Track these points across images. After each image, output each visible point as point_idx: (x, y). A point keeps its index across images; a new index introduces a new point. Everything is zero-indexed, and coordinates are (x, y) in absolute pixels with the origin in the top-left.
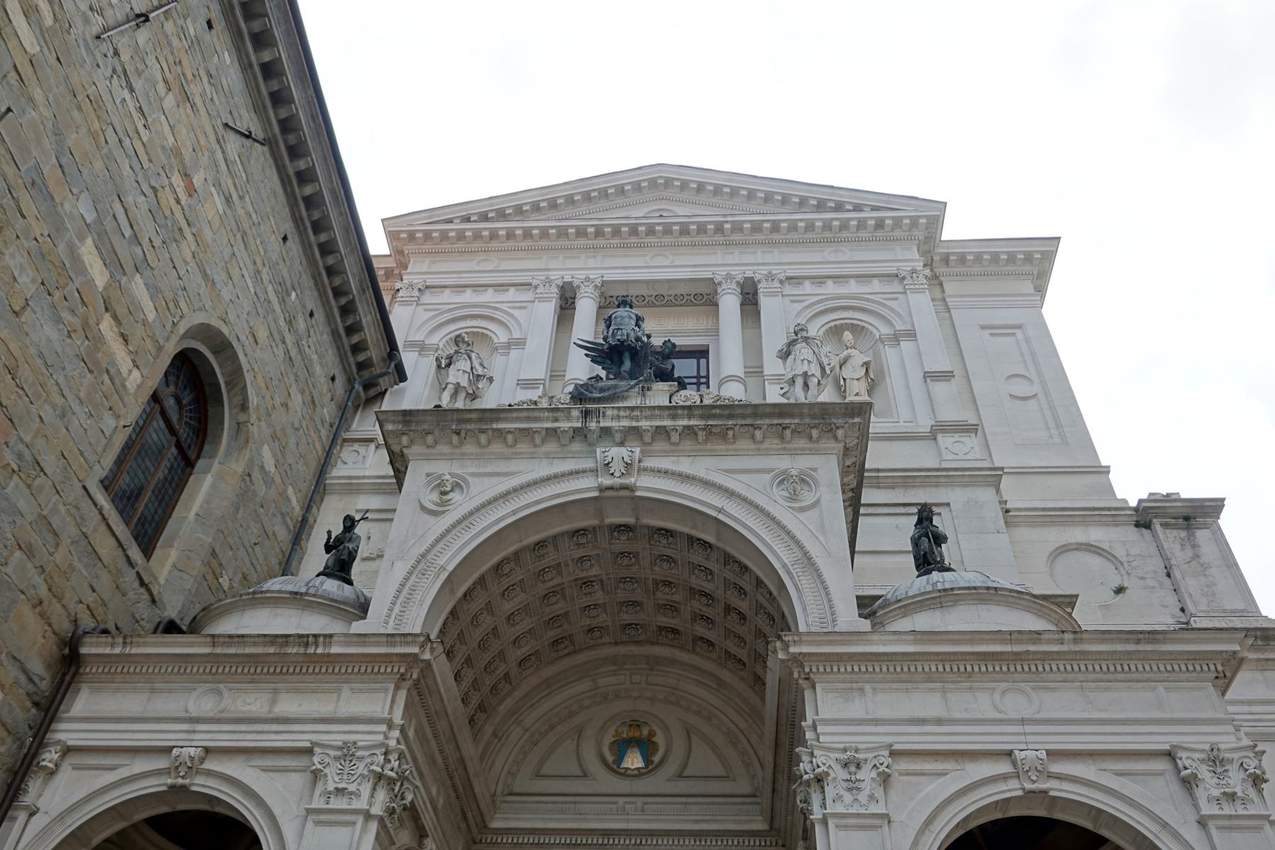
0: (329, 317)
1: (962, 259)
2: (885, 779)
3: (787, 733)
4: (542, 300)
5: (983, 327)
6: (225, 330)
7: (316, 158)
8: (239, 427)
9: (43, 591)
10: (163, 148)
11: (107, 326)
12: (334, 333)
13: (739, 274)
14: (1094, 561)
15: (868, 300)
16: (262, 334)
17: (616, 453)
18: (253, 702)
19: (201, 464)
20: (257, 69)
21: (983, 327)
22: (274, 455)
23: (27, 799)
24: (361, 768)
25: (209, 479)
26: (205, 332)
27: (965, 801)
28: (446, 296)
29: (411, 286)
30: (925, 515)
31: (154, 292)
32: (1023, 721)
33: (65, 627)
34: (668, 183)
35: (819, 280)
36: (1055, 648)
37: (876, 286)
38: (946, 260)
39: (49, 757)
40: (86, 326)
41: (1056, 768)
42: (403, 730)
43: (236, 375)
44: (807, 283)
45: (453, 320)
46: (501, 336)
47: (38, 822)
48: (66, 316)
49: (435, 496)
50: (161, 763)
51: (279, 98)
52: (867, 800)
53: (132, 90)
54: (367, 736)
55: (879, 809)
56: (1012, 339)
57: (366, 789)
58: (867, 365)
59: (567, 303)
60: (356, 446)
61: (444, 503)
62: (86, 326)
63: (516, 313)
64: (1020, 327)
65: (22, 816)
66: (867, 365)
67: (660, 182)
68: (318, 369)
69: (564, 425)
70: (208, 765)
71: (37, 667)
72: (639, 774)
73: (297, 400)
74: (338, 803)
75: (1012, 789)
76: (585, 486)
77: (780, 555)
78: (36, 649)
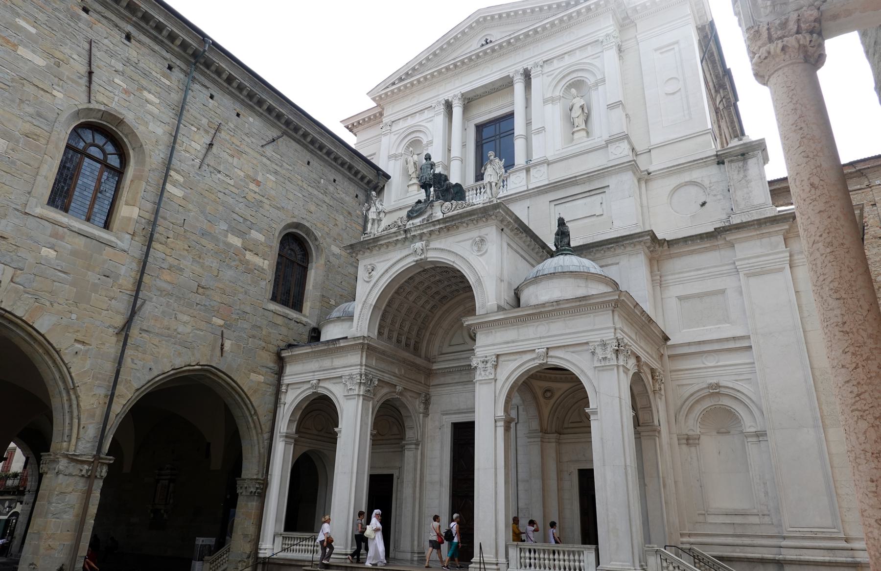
0: (344, 175)
2: (496, 367)
4: (437, 115)
5: (656, 50)
6: (295, 220)
7: (305, 127)
8: (317, 247)
9: (264, 344)
10: (241, 180)
11: (249, 256)
12: (350, 179)
13: (520, 68)
14: (693, 190)
15: (584, 63)
16: (313, 208)
17: (419, 245)
20: (264, 113)
21: (656, 50)
22: (338, 246)
23: (282, 401)
25: (313, 271)
26: (289, 226)
27: (516, 373)
28: (402, 125)
30: (561, 223)
31: (260, 231)
32: (540, 338)
33: (276, 349)
34: (485, 18)
35: (561, 57)
36: (550, 308)
38: (635, 10)
39: (284, 388)
40: (241, 261)
42: (366, 366)
43: (308, 231)
44: (555, 61)
45: (406, 137)
46: (425, 142)
47: (287, 406)
48: (233, 264)
49: (367, 275)
51: (279, 116)
53: (219, 172)
55: (492, 377)
57: (357, 387)
58: (582, 107)
61: (370, 277)
62: (241, 261)
63: (428, 125)
64: (677, 42)
65: (282, 406)
66: (582, 107)
68: (347, 199)
69: (399, 238)
70: (321, 384)
71: (271, 365)
73: (340, 218)
74: (351, 393)
75: (537, 362)
76: (410, 261)
78: (268, 359)
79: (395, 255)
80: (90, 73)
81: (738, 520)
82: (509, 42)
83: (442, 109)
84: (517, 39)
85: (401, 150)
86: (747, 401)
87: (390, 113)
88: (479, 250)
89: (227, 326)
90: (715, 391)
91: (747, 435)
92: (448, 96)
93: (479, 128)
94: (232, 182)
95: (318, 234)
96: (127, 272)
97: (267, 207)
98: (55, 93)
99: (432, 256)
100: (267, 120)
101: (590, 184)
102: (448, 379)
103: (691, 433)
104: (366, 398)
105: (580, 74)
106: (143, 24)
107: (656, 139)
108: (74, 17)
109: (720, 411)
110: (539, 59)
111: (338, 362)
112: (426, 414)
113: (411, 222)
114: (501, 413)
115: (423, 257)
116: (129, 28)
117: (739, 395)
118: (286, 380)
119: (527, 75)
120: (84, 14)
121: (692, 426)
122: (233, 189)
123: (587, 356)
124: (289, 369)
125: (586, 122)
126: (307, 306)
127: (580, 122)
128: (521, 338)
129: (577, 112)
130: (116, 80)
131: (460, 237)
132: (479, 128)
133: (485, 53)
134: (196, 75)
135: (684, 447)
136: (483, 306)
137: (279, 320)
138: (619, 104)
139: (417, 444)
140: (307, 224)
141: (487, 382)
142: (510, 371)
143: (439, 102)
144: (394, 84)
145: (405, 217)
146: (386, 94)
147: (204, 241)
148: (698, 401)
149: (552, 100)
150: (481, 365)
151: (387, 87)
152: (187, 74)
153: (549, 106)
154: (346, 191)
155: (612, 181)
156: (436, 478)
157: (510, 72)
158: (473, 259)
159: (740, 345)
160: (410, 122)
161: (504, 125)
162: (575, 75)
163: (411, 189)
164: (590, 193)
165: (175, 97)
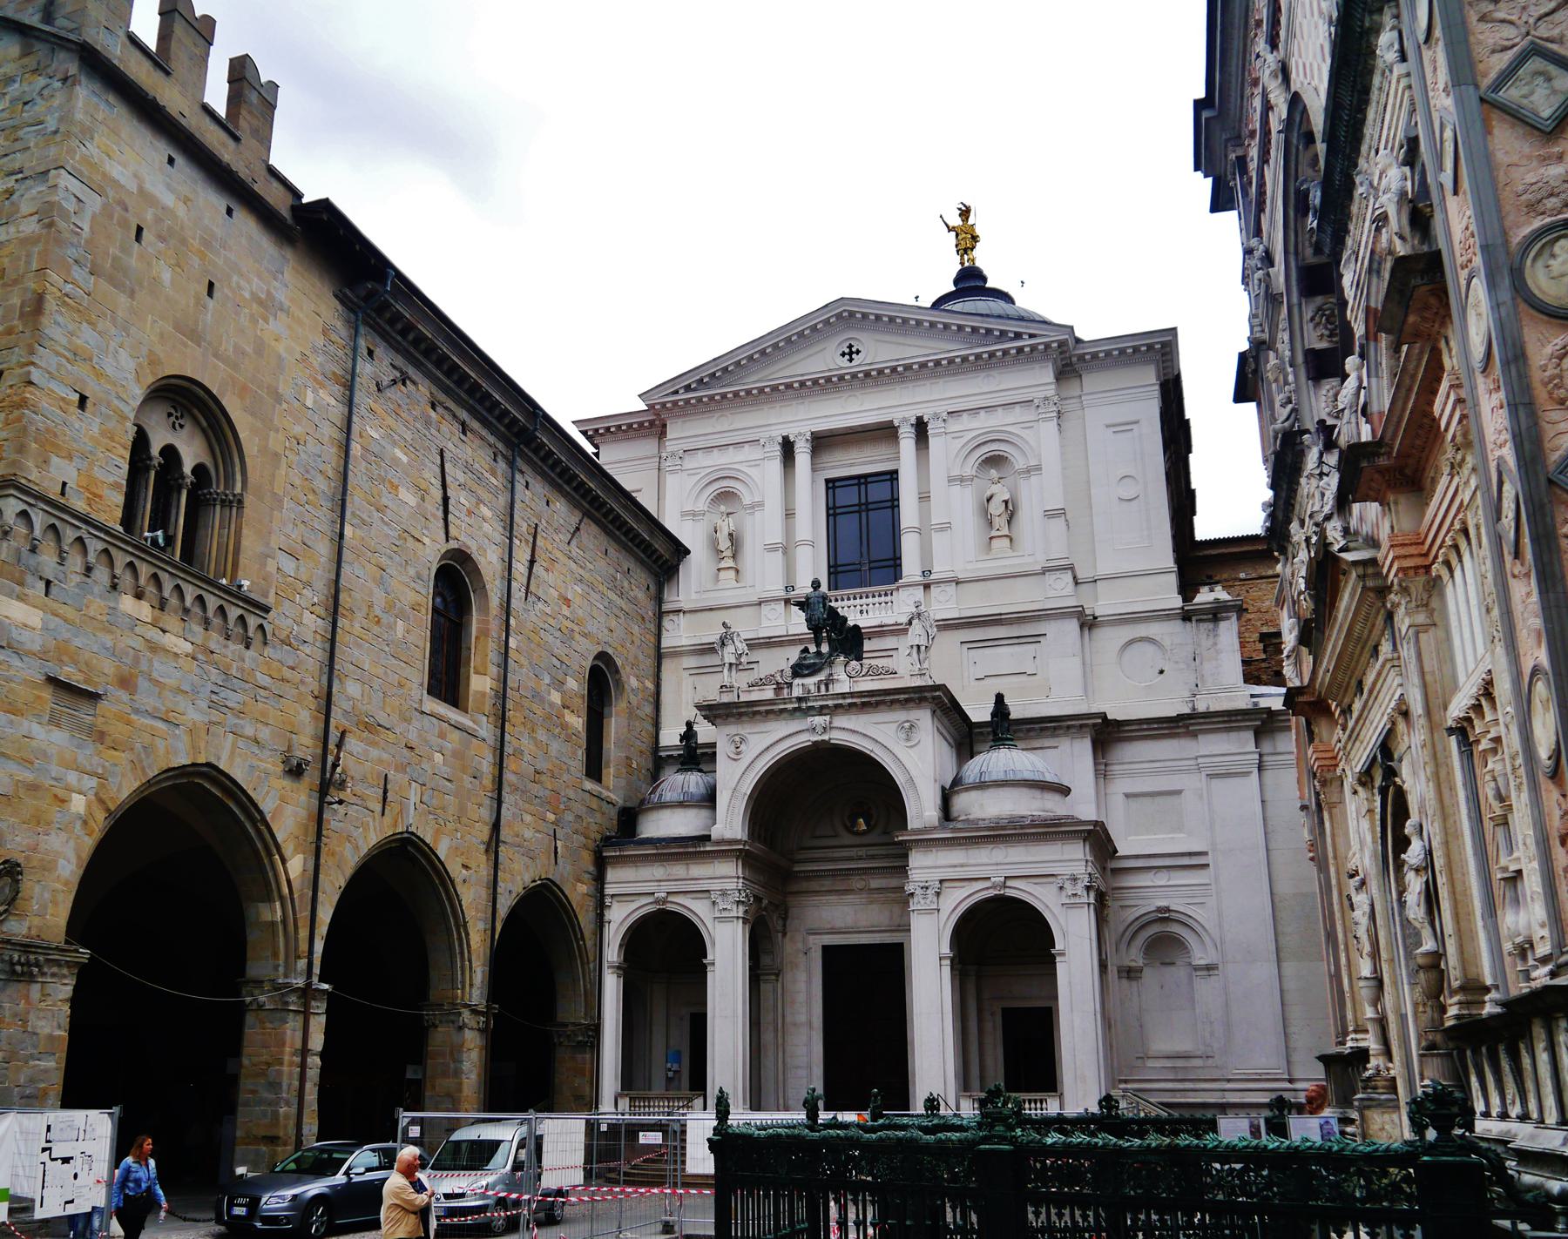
1: (1095, 356)
2: (938, 894)
3: (902, 870)
4: (769, 458)
8: (619, 684)
13: (912, 414)
14: (1149, 649)
17: (819, 720)
18: (678, 870)
19: (606, 711)
24: (731, 899)
28: (701, 460)
29: (673, 455)
30: (1000, 698)
34: (852, 314)
37: (1018, 414)
38: (1081, 358)
39: (608, 901)
41: (1009, 883)
46: (747, 500)
47: (613, 926)
50: (651, 899)
52: (930, 902)
54: (731, 885)
56: (1129, 434)
58: (1006, 502)
59: (788, 447)
60: (671, 616)
63: (752, 472)
66: (1006, 502)
67: (847, 318)
72: (864, 833)
73: (636, 629)
77: (899, 778)
80: (446, 499)
81: (1180, 1063)
82: (894, 370)
83: (777, 450)
84: (908, 367)
85: (702, 505)
86: (1198, 928)
87: (678, 432)
88: (908, 740)
90: (1164, 916)
91: (1197, 968)
92: (791, 431)
93: (831, 484)
94: (548, 610)
95: (619, 662)
96: (486, 766)
97: (577, 636)
98: (426, 540)
99: (837, 737)
101: (1016, 626)
102: (814, 885)
103: (1133, 964)
104: (745, 921)
105: (1003, 447)
106: (478, 407)
107: (1103, 569)
108: (428, 423)
109: (1163, 939)
110: (942, 409)
111: (697, 870)
112: (784, 934)
113: (798, 681)
114: (946, 950)
115: (826, 737)
116: (464, 415)
117: (1190, 922)
118: (609, 890)
119: (921, 428)
120: (433, 414)
121: (1135, 957)
122: (551, 621)
123: (1054, 889)
124: (612, 874)
125: (1009, 522)
126: (610, 773)
127: (999, 522)
128: (972, 862)
129: (996, 508)
130: (462, 500)
132: (831, 484)
133: (854, 376)
134: (520, 462)
135: (1124, 981)
136: (920, 816)
137: (594, 804)
138: (1061, 513)
139: (777, 975)
140: (610, 651)
141: (929, 912)
142: (956, 901)
143: (771, 439)
144: (688, 388)
145: (788, 672)
146: (675, 403)
147: (535, 707)
148: (1143, 927)
149: (962, 479)
150: (919, 892)
151: (676, 392)
152: (511, 464)
153: (956, 489)
154: (638, 584)
155: (1050, 628)
156: (803, 1018)
157: (896, 416)
158: (899, 749)
159: (1193, 862)
162: (994, 446)
163: (723, 574)
164: (1020, 640)
165: (503, 500)
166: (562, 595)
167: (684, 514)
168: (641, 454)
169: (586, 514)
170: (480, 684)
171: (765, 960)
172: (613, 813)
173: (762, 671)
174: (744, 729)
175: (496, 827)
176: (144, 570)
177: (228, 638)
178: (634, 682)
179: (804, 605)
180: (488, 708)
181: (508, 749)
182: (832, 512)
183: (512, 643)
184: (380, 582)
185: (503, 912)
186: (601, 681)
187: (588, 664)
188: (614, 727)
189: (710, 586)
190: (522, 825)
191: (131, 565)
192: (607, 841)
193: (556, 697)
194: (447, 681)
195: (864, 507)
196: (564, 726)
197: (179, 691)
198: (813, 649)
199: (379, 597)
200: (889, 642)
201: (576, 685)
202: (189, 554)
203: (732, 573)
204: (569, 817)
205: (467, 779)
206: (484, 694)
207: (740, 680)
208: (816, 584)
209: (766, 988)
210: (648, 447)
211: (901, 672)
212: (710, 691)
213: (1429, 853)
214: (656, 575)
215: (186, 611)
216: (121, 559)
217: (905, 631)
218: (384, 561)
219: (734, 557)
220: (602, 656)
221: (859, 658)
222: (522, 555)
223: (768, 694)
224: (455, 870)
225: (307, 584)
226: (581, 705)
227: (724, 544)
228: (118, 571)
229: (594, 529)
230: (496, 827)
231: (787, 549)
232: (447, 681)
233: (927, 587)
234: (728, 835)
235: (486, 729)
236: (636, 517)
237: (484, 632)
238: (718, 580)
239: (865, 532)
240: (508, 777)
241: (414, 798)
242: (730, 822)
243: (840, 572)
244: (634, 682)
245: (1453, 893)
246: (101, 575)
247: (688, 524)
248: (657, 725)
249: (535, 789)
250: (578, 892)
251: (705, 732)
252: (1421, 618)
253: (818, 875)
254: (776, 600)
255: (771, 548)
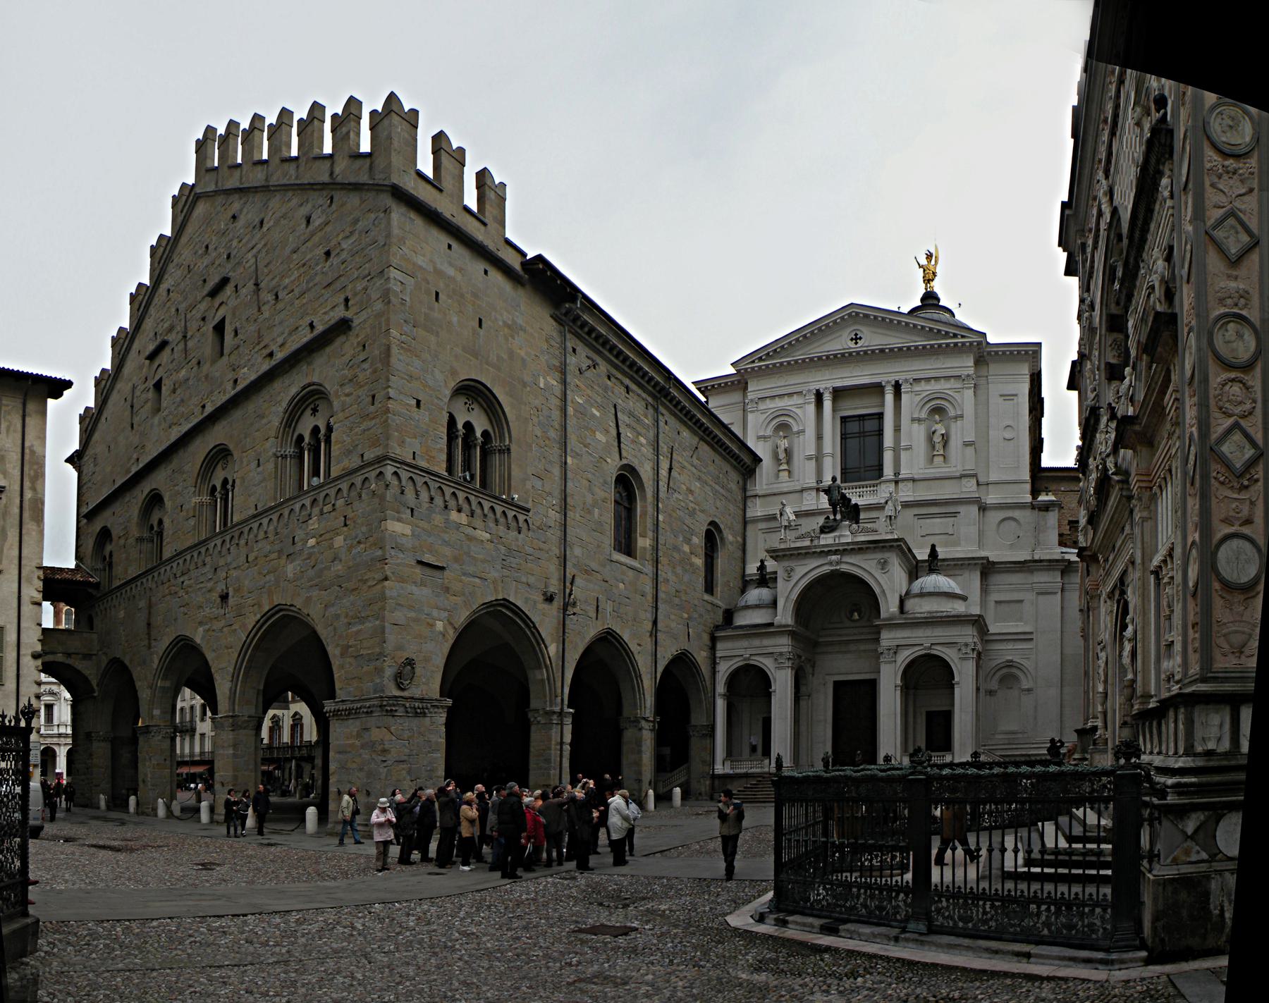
8: (722, 539)
17: (834, 557)
18: (756, 642)
46: (795, 429)
59: (819, 397)
63: (798, 411)
76: (827, 569)
78: (706, 638)
79: (814, 563)
83: (812, 398)
85: (769, 432)
89: (689, 618)
95: (722, 526)
96: (649, 589)
100: (695, 433)
111: (766, 642)
118: (719, 654)
124: (719, 646)
126: (718, 589)
131: (867, 556)
137: (709, 607)
147: (675, 554)
160: (779, 403)
161: (870, 425)
163: (781, 474)
166: (687, 488)
167: (759, 438)
168: (733, 401)
169: (702, 439)
170: (643, 543)
171: (803, 689)
172: (720, 612)
173: (803, 530)
174: (792, 564)
175: (655, 623)
176: (461, 496)
177: (509, 528)
178: (730, 538)
179: (828, 491)
180: (648, 556)
181: (660, 579)
182: (844, 437)
183: (661, 518)
184: (590, 490)
185: (660, 669)
186: (712, 537)
187: (705, 528)
188: (721, 562)
189: (773, 480)
190: (670, 620)
191: (454, 494)
192: (717, 628)
193: (686, 548)
194: (626, 544)
195: (862, 434)
196: (692, 565)
197: (484, 561)
198: (832, 517)
199: (589, 499)
200: (874, 514)
201: (698, 541)
202: (484, 483)
203: (786, 473)
204: (696, 616)
205: (638, 597)
206: (645, 549)
207: (791, 535)
208: (834, 479)
209: (803, 703)
210: (736, 397)
211: (880, 531)
212: (775, 541)
213: (1135, 632)
214: (743, 475)
215: (485, 516)
216: (448, 491)
217: (883, 508)
218: (590, 476)
219: (788, 463)
220: (712, 523)
221: (857, 522)
222: (664, 465)
223: (807, 543)
224: (633, 647)
225: (550, 494)
226: (701, 552)
227: (782, 455)
228: (447, 498)
229: (706, 448)
230: (655, 623)
231: (818, 458)
232: (626, 544)
233: (897, 482)
234: (784, 622)
235: (649, 569)
236: (731, 439)
237: (644, 513)
238: (777, 476)
239: (862, 447)
240: (661, 595)
241: (609, 609)
242: (785, 616)
243: (847, 474)
244: (730, 538)
245: (1143, 651)
246: (439, 501)
247: (761, 443)
248: (744, 562)
249: (677, 601)
250: (701, 657)
251: (771, 565)
252: (1145, 514)
253: (831, 644)
254: (810, 489)
255: (809, 458)
